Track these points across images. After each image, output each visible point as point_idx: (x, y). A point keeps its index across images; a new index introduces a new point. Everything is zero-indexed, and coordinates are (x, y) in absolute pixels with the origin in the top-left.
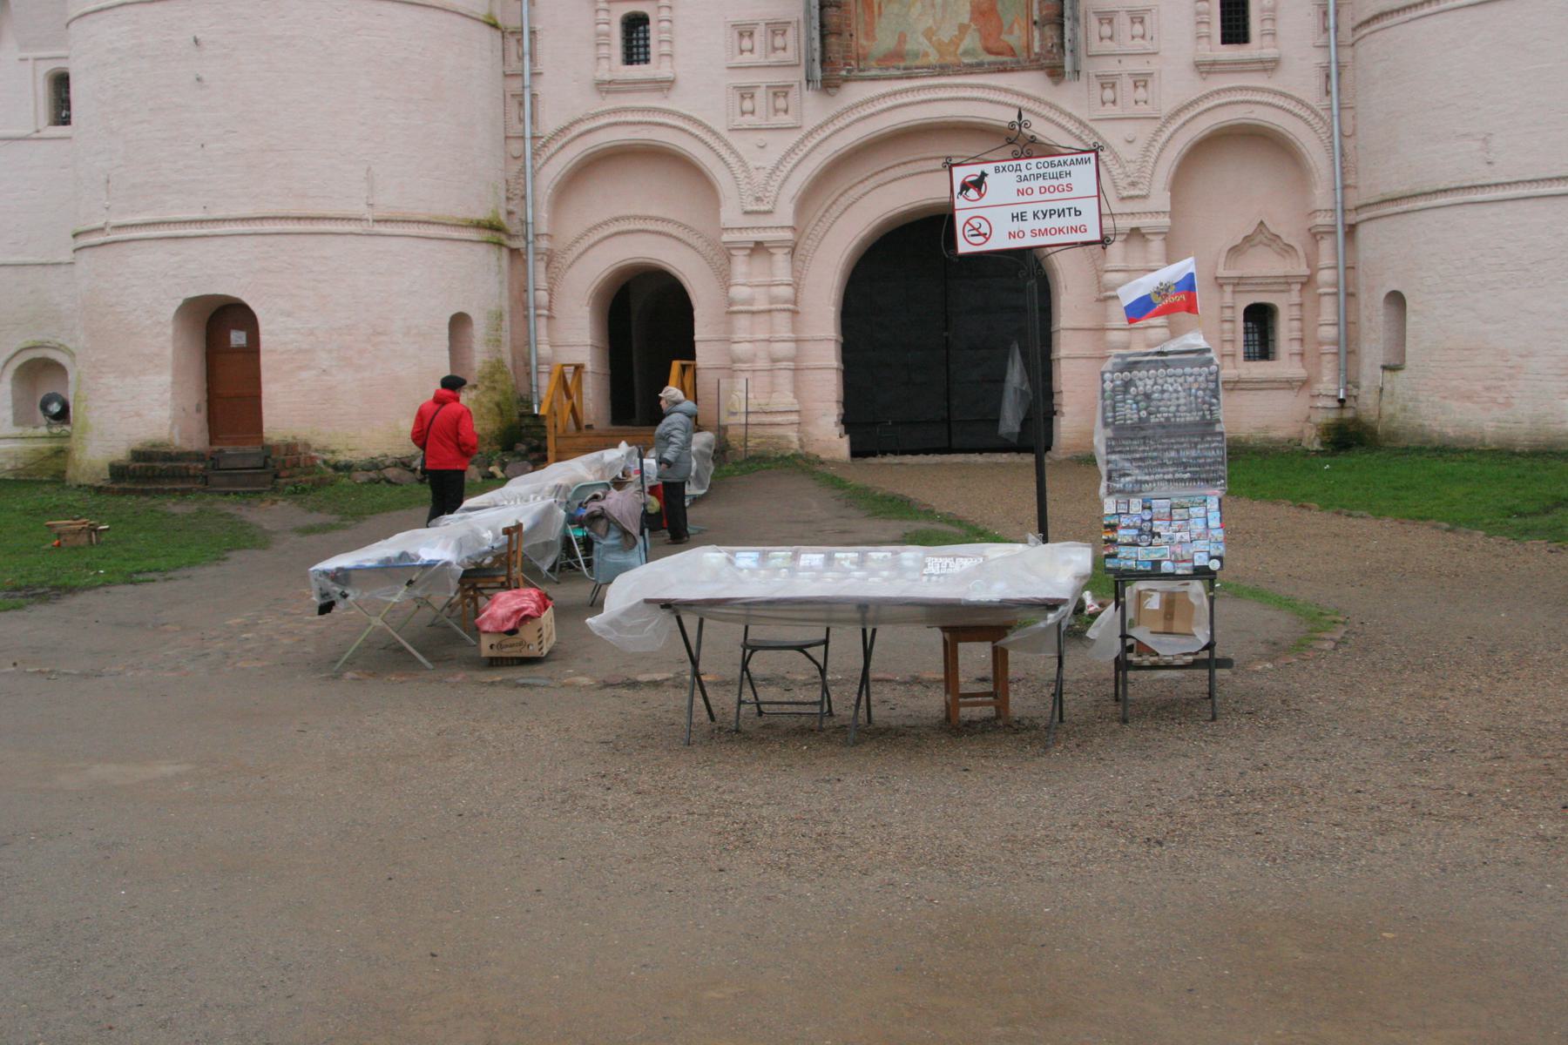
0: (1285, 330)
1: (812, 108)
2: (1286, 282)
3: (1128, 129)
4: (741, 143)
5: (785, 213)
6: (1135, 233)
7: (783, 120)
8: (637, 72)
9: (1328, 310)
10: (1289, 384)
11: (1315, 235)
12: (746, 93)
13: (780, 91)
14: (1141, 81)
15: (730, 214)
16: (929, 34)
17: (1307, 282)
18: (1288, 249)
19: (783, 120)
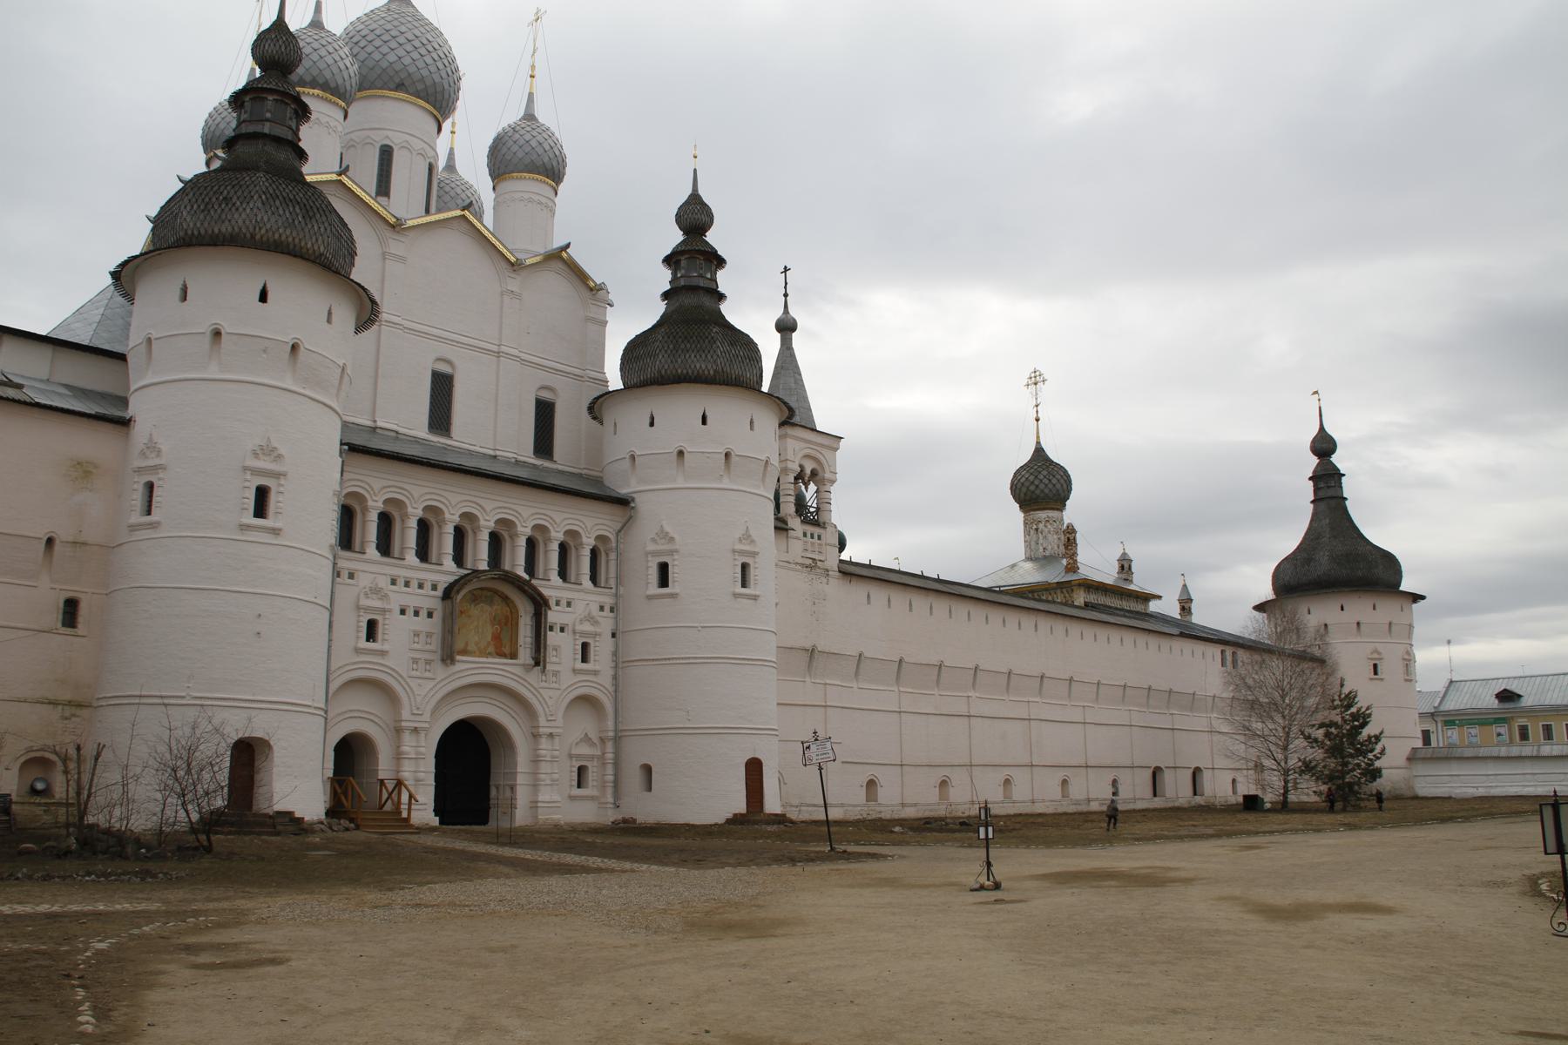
0: (591, 776)
1: (440, 672)
2: (592, 757)
3: (551, 693)
4: (413, 683)
5: (427, 717)
6: (551, 735)
7: (427, 674)
8: (371, 645)
9: (610, 770)
10: (592, 798)
11: (602, 740)
12: (415, 661)
13: (428, 662)
14: (556, 673)
15: (405, 714)
16: (477, 644)
17: (602, 757)
18: (593, 744)
19: (427, 674)
